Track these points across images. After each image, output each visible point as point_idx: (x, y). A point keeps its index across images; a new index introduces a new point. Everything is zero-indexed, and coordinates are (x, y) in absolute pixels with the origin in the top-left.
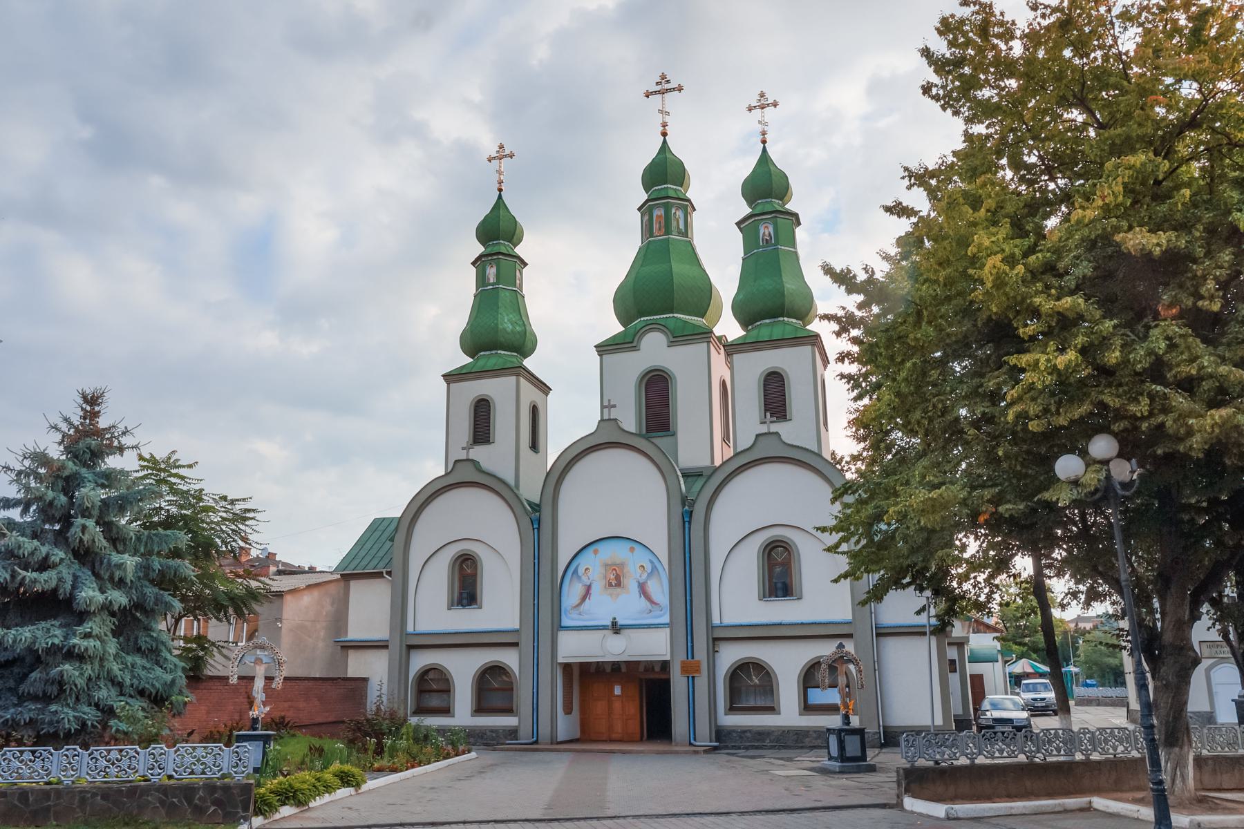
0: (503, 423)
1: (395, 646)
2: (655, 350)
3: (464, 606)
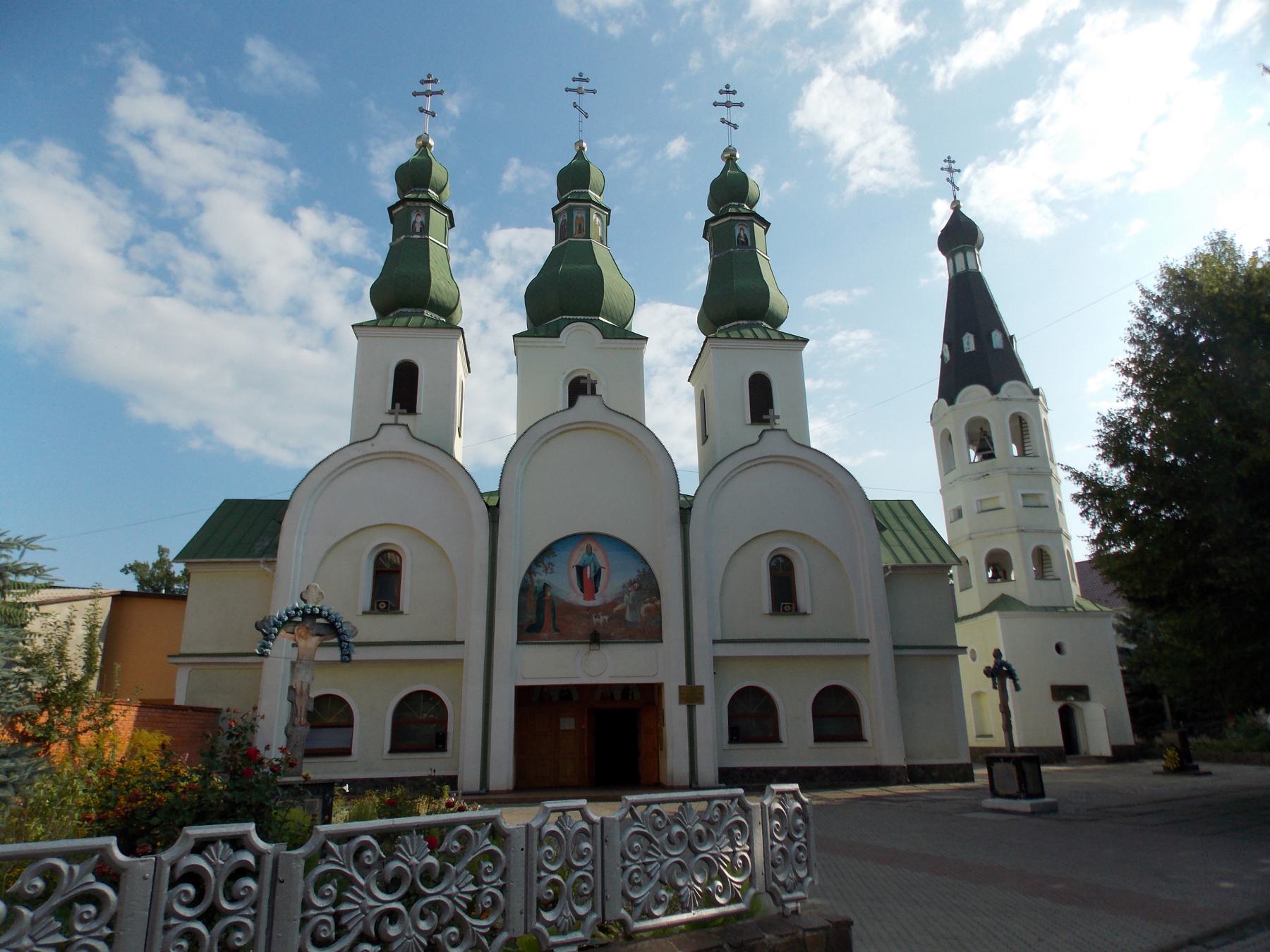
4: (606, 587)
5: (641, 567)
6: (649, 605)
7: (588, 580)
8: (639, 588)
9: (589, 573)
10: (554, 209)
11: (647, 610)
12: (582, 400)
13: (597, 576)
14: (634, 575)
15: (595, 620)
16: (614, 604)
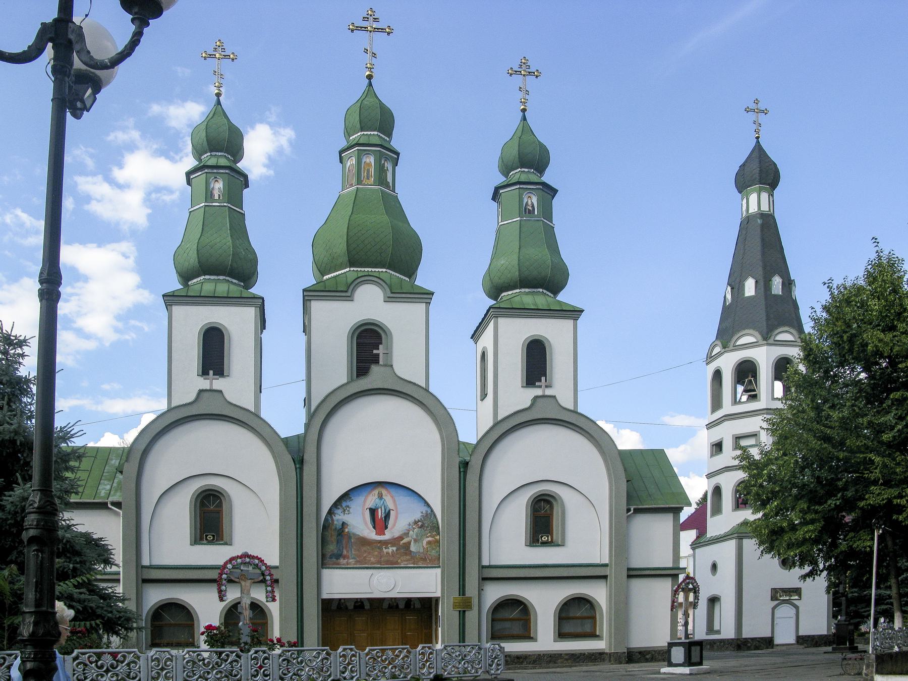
0: (239, 354)
4: (394, 525)
5: (425, 509)
6: (430, 539)
7: (380, 520)
9: (380, 514)
11: (429, 543)
12: (374, 368)
13: (387, 516)
14: (418, 516)
15: (385, 551)
16: (401, 538)
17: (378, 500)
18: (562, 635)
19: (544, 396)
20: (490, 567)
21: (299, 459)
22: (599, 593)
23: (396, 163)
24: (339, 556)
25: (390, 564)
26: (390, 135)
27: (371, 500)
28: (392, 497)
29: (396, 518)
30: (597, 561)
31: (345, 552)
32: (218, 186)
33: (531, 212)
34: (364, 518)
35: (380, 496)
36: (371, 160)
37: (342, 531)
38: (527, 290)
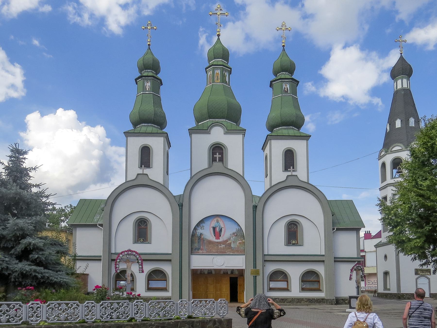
1: (106, 259)
2: (217, 135)
3: (142, 243)
4: (224, 235)
6: (240, 241)
7: (217, 233)
8: (236, 235)
9: (217, 230)
10: (206, 69)
11: (240, 243)
13: (221, 230)
14: (235, 231)
16: (227, 241)
17: (216, 223)
18: (303, 290)
19: (292, 175)
20: (268, 255)
21: (181, 205)
22: (320, 269)
23: (230, 73)
24: (198, 249)
25: (222, 253)
26: (227, 60)
27: (213, 223)
28: (223, 222)
29: (225, 231)
30: (319, 253)
31: (202, 247)
32: (148, 85)
33: (287, 92)
34: (210, 231)
35: (218, 222)
36: (218, 72)
37: (200, 237)
38: (285, 127)
